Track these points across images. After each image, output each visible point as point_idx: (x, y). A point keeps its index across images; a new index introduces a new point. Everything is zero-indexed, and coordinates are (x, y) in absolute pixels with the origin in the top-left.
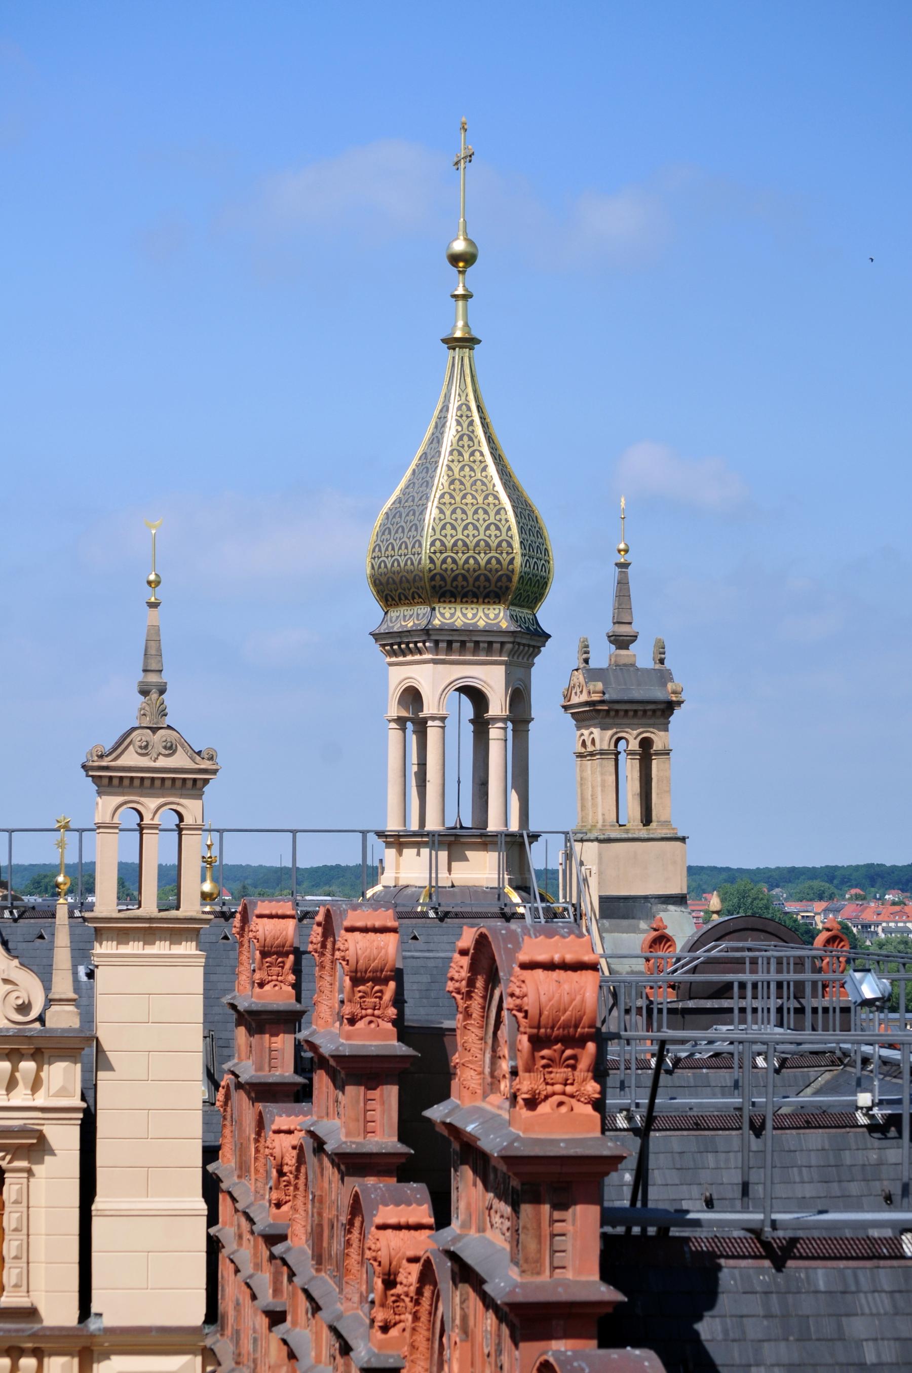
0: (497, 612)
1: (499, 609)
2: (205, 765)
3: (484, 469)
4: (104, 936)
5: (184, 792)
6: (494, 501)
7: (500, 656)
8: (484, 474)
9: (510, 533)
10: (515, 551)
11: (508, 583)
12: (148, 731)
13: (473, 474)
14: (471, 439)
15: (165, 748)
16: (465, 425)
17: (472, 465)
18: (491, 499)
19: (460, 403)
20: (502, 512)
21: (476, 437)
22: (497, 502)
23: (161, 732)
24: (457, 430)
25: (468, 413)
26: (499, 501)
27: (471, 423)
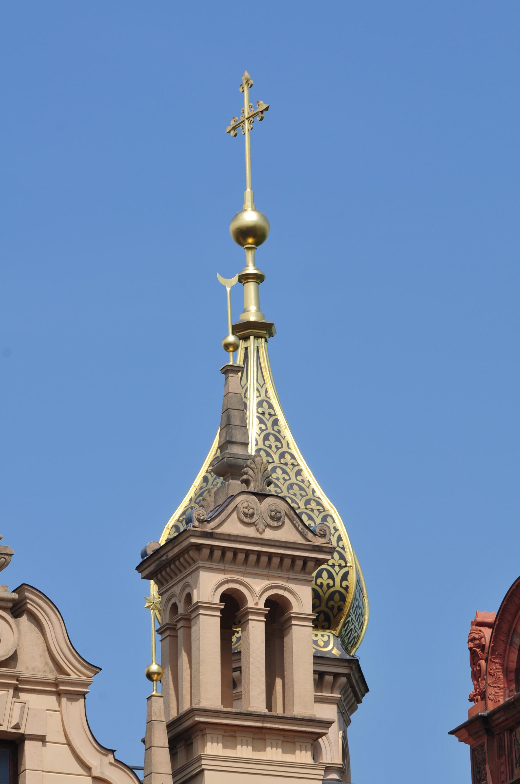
0: (326, 638)
1: (329, 636)
2: (319, 541)
3: (299, 473)
4: (209, 737)
5: (293, 575)
6: (318, 507)
7: (332, 693)
8: (299, 478)
9: (341, 544)
10: (348, 565)
11: (341, 603)
12: (254, 498)
13: (287, 478)
14: (277, 439)
15: (273, 518)
16: (269, 424)
17: (284, 467)
18: (313, 505)
19: (260, 399)
20: (329, 519)
21: (284, 438)
22: (321, 508)
23: (269, 500)
24: (260, 428)
25: (271, 411)
26: (323, 507)
27: (276, 422)
